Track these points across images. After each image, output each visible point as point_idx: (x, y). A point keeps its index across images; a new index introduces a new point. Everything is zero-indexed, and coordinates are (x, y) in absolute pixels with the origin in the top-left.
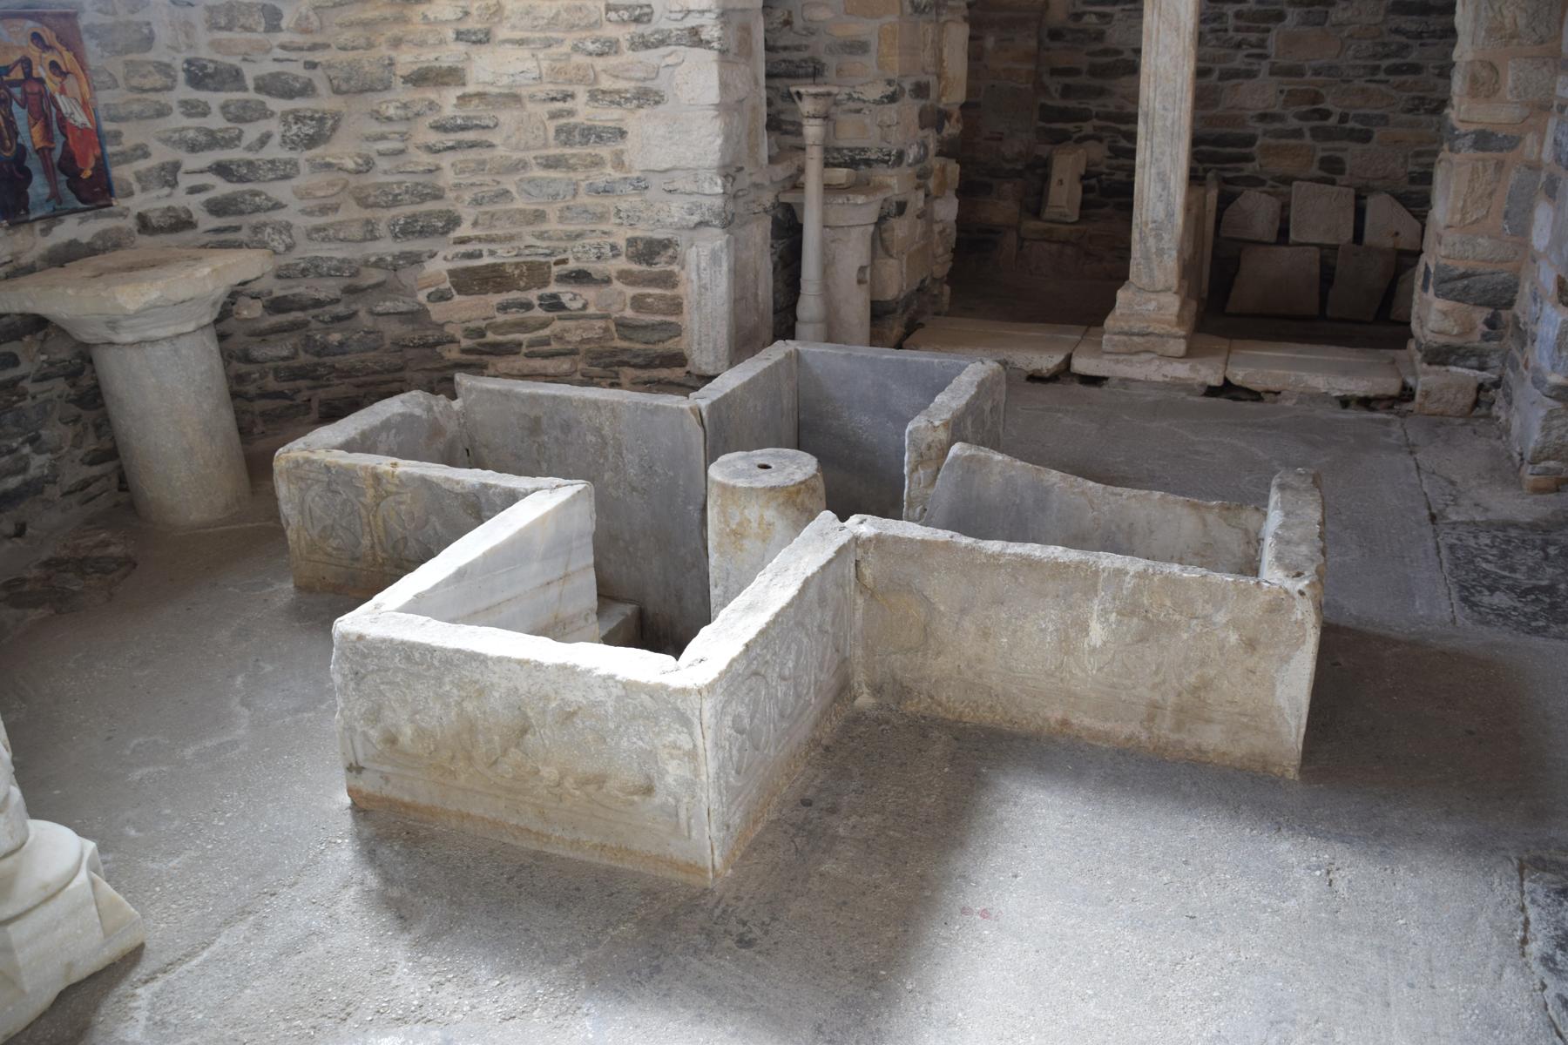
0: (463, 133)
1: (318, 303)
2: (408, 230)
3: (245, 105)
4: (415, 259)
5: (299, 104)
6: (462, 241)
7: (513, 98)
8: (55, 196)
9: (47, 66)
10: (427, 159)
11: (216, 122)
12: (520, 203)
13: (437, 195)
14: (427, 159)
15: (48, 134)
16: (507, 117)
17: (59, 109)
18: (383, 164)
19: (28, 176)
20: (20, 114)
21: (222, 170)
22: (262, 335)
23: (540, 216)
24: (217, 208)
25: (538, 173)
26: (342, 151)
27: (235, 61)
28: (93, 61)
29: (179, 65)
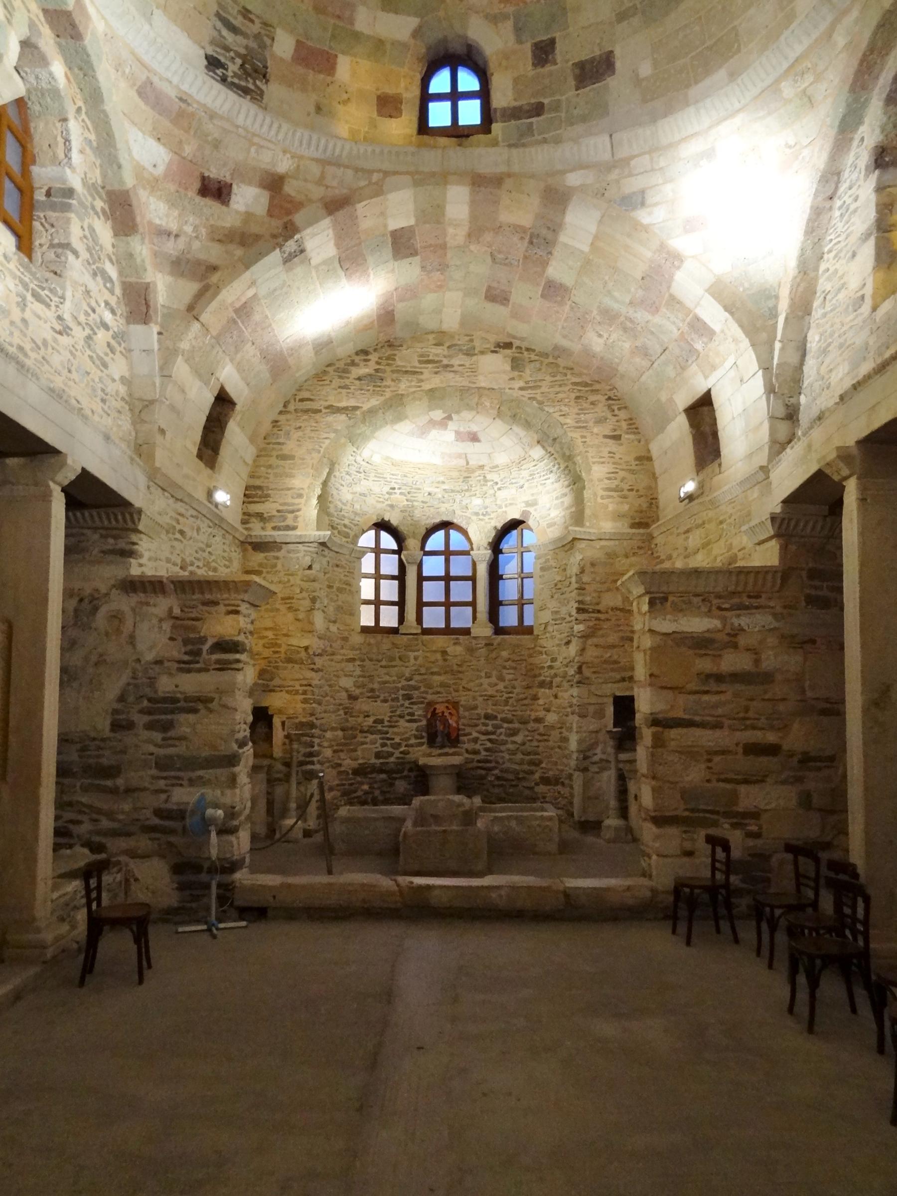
0: (544, 736)
4: (532, 773)
5: (510, 725)
6: (542, 768)
7: (553, 727)
11: (490, 728)
13: (538, 754)
15: (444, 727)
16: (553, 733)
18: (528, 743)
21: (490, 740)
22: (494, 786)
23: (556, 763)
24: (487, 750)
25: (557, 750)
26: (519, 739)
27: (495, 713)
28: (461, 712)
29: (483, 714)
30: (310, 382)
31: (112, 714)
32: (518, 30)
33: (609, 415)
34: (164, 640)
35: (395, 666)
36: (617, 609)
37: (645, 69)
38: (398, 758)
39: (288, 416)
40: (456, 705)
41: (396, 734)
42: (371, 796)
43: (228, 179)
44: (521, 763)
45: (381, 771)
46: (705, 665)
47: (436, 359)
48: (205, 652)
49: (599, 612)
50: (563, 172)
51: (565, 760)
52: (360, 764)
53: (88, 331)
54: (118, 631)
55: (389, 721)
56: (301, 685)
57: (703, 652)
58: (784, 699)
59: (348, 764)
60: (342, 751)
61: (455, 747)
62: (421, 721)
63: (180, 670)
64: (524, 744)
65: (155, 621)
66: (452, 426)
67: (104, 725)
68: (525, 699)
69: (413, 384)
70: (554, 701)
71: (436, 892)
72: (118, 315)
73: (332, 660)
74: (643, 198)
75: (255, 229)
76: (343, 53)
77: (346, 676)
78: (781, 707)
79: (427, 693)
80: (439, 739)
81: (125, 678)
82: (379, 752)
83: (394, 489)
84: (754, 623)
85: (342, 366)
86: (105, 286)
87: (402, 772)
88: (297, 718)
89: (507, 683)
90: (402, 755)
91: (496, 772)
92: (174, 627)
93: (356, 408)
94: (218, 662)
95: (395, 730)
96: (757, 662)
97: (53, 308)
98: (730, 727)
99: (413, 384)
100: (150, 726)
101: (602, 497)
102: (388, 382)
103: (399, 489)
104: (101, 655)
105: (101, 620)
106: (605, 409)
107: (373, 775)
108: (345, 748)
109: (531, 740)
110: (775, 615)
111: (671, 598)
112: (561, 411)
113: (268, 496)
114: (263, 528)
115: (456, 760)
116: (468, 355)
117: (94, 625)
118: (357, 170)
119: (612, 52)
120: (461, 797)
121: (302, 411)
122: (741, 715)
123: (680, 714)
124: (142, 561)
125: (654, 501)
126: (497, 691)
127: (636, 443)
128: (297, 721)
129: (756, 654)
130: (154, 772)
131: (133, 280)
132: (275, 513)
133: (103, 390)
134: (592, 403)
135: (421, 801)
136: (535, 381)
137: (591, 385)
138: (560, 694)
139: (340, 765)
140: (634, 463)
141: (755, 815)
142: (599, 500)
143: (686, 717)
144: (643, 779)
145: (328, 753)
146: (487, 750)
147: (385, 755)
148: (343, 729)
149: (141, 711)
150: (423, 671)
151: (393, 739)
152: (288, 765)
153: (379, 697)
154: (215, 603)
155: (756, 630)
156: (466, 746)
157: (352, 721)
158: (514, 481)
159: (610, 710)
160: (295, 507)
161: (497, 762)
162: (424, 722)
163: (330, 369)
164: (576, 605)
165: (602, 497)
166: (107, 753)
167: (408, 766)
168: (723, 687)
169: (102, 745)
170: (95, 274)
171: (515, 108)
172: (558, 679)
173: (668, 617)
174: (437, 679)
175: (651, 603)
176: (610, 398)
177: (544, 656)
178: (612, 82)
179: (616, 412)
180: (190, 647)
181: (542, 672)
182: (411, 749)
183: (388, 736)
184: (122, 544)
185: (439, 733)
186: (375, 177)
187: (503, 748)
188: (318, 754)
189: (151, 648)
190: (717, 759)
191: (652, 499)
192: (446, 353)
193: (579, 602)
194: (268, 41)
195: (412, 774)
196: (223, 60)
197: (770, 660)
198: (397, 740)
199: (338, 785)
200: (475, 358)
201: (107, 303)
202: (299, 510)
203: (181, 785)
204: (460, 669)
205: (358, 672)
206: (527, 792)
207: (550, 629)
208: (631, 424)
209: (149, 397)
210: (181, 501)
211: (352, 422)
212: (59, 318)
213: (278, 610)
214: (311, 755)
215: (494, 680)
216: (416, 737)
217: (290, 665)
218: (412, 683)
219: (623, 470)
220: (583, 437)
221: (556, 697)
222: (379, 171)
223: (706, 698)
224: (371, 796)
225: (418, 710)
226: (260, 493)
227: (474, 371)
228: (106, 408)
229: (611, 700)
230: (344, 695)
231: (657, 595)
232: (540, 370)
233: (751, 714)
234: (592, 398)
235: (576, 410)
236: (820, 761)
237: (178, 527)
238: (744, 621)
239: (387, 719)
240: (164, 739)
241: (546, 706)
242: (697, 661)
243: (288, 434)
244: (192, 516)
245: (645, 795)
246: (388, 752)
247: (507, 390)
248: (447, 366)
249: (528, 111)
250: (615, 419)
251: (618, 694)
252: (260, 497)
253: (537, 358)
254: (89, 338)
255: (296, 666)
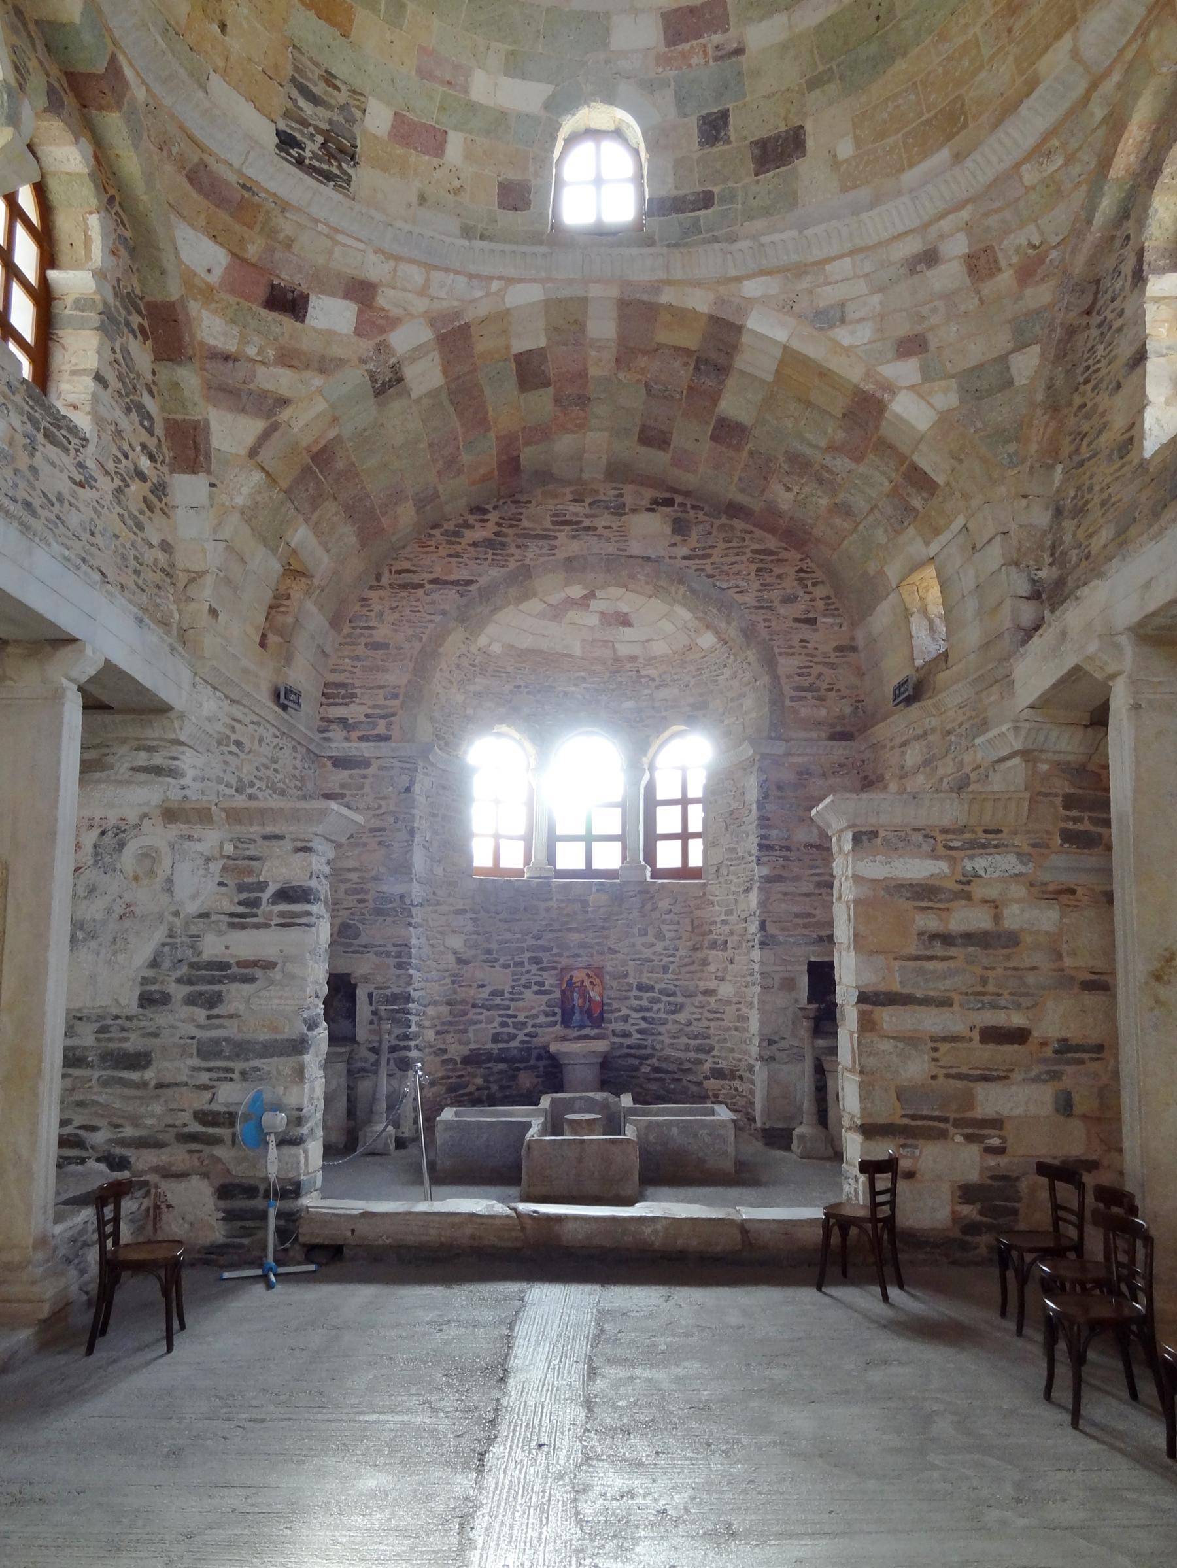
1: (668, 1072)
2: (698, 1050)
3: (653, 998)
4: (700, 1062)
5: (671, 999)
7: (728, 1003)
8: (582, 1020)
10: (707, 1023)
11: (645, 1003)
12: (729, 1045)
14: (707, 1023)
15: (584, 1002)
16: (727, 1009)
18: (695, 1023)
20: (576, 995)
21: (644, 1019)
22: (649, 1080)
23: (732, 1050)
24: (640, 1032)
26: (682, 1017)
30: (409, 549)
31: (142, 984)
32: (680, 101)
33: (801, 593)
34: (211, 886)
35: (520, 920)
36: (812, 846)
37: (846, 149)
38: (522, 1042)
39: (382, 593)
40: (599, 972)
41: (517, 1009)
42: (486, 1092)
43: (304, 288)
44: (687, 1049)
45: (500, 1060)
46: (931, 923)
47: (575, 519)
48: (264, 901)
49: (788, 849)
50: (739, 279)
51: (744, 1046)
52: (471, 1050)
53: (118, 482)
54: (151, 873)
55: (511, 993)
56: (394, 945)
57: (925, 904)
58: (1034, 968)
59: (457, 1050)
60: (447, 1032)
61: (599, 1027)
62: (550, 992)
63: (232, 925)
64: (689, 1024)
65: (200, 861)
66: (595, 605)
67: (129, 1000)
68: (693, 963)
69: (544, 551)
70: (730, 967)
71: (570, 1226)
72: (159, 461)
73: (436, 912)
74: (843, 312)
75: (337, 351)
76: (456, 129)
77: (454, 932)
78: (1031, 979)
79: (561, 955)
80: (577, 1017)
81: (160, 935)
82: (498, 1034)
83: (519, 687)
84: (994, 867)
85: (452, 528)
86: (142, 424)
87: (528, 1061)
88: (389, 988)
89: (668, 942)
90: (527, 1039)
91: (654, 1061)
92: (225, 869)
93: (469, 583)
94: (282, 914)
95: (520, 1004)
96: (997, 918)
97: (72, 452)
98: (961, 1005)
99: (544, 551)
100: (191, 1000)
101: (792, 699)
102: (512, 549)
103: (526, 687)
104: (128, 905)
105: (128, 858)
106: (795, 583)
107: (489, 1065)
108: (452, 1028)
109: (699, 1020)
110: (1019, 855)
111: (882, 834)
112: (737, 586)
113: (353, 696)
114: (347, 739)
115: (601, 1046)
116: (616, 514)
117: (118, 867)
118: (471, 276)
119: (802, 127)
120: (605, 1094)
121: (399, 585)
122: (979, 989)
123: (897, 987)
124: (183, 782)
125: (859, 705)
126: (654, 953)
127: (836, 628)
128: (388, 992)
129: (996, 907)
130: (195, 1062)
131: (179, 417)
132: (363, 719)
133: (136, 558)
134: (779, 577)
135: (553, 1100)
136: (704, 548)
137: (777, 553)
138: (737, 958)
139: (445, 1051)
140: (833, 655)
141: (996, 1123)
142: (788, 703)
143: (904, 991)
144: (846, 1074)
145: (430, 1035)
146: (640, 1032)
147: (506, 1038)
148: (449, 1003)
149: (179, 981)
150: (556, 926)
151: (516, 1017)
152: (375, 1050)
153: (497, 960)
154: (280, 837)
155: (996, 875)
156: (613, 1026)
157: (462, 994)
158: (676, 677)
159: (804, 981)
160: (390, 711)
161: (653, 1048)
162: (558, 995)
163: (437, 532)
164: (757, 841)
165: (792, 699)
166: (133, 1036)
167: (535, 1053)
168: (952, 952)
169: (128, 1024)
170: (128, 410)
171: (675, 199)
172: (736, 938)
173: (879, 858)
174: (575, 937)
175: (857, 839)
176: (801, 570)
177: (717, 908)
178: (802, 165)
179: (810, 588)
180: (244, 896)
181: (713, 928)
182: (539, 1030)
183: (509, 1012)
184: (158, 760)
185: (577, 1009)
186: (495, 286)
187: (662, 1029)
188: (416, 1036)
189: (193, 898)
190: (944, 1047)
191: (859, 701)
192: (588, 511)
193: (763, 837)
194: (358, 114)
195: (541, 1064)
196: (299, 137)
197: (1015, 917)
198: (521, 1018)
199: (442, 1078)
200: (624, 518)
201: (144, 446)
202: (393, 715)
203: (231, 1079)
204: (607, 925)
205: (470, 927)
206: (694, 1088)
207: (724, 871)
208: (829, 604)
209: (197, 568)
210: (238, 702)
211: (464, 600)
212: (80, 465)
213: (365, 845)
214: (406, 1037)
215: (650, 938)
216: (547, 1015)
217: (381, 918)
218: (540, 942)
219: (817, 663)
220: (765, 620)
221: (732, 962)
222: (499, 278)
223: (930, 965)
224: (486, 1092)
225: (549, 979)
226: (343, 692)
227: (623, 534)
228: (140, 582)
229: (805, 968)
230: (451, 959)
231: (864, 829)
232: (710, 533)
233: (990, 988)
234: (777, 570)
235: (756, 585)
236: (1084, 1051)
237: (233, 737)
238: (980, 863)
239: (507, 989)
240: (209, 1017)
241: (719, 974)
242: (917, 918)
243: (381, 614)
244: (253, 723)
245: (849, 1098)
246: (509, 1034)
247: (667, 559)
248: (588, 529)
249: (693, 202)
250: (807, 597)
251: (813, 959)
252: (343, 698)
253: (706, 518)
254: (119, 491)
255: (388, 919)
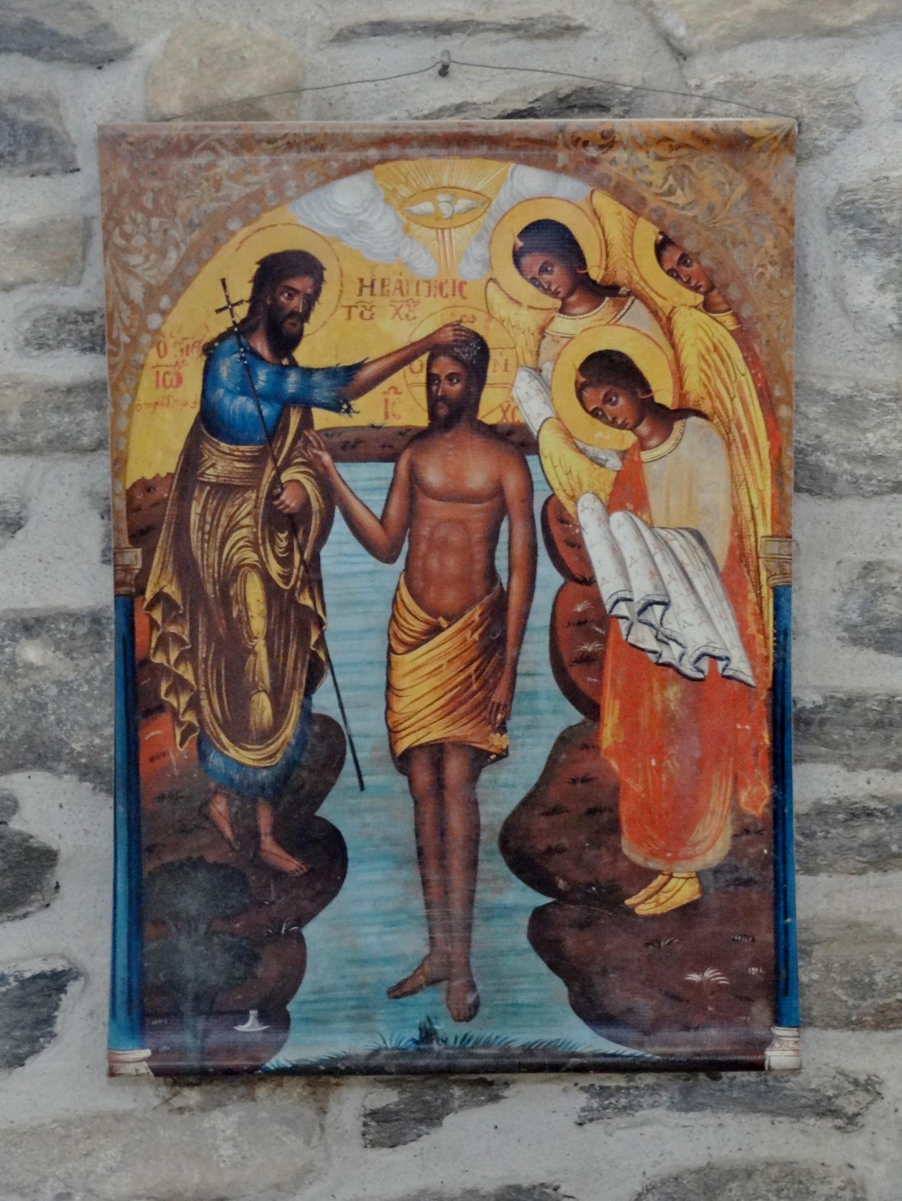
8: (447, 971)
9: (566, 374)
17: (580, 577)
19: (326, 859)
20: (356, 585)
80: (365, 927)
